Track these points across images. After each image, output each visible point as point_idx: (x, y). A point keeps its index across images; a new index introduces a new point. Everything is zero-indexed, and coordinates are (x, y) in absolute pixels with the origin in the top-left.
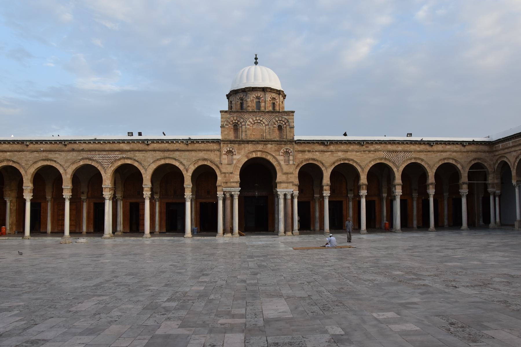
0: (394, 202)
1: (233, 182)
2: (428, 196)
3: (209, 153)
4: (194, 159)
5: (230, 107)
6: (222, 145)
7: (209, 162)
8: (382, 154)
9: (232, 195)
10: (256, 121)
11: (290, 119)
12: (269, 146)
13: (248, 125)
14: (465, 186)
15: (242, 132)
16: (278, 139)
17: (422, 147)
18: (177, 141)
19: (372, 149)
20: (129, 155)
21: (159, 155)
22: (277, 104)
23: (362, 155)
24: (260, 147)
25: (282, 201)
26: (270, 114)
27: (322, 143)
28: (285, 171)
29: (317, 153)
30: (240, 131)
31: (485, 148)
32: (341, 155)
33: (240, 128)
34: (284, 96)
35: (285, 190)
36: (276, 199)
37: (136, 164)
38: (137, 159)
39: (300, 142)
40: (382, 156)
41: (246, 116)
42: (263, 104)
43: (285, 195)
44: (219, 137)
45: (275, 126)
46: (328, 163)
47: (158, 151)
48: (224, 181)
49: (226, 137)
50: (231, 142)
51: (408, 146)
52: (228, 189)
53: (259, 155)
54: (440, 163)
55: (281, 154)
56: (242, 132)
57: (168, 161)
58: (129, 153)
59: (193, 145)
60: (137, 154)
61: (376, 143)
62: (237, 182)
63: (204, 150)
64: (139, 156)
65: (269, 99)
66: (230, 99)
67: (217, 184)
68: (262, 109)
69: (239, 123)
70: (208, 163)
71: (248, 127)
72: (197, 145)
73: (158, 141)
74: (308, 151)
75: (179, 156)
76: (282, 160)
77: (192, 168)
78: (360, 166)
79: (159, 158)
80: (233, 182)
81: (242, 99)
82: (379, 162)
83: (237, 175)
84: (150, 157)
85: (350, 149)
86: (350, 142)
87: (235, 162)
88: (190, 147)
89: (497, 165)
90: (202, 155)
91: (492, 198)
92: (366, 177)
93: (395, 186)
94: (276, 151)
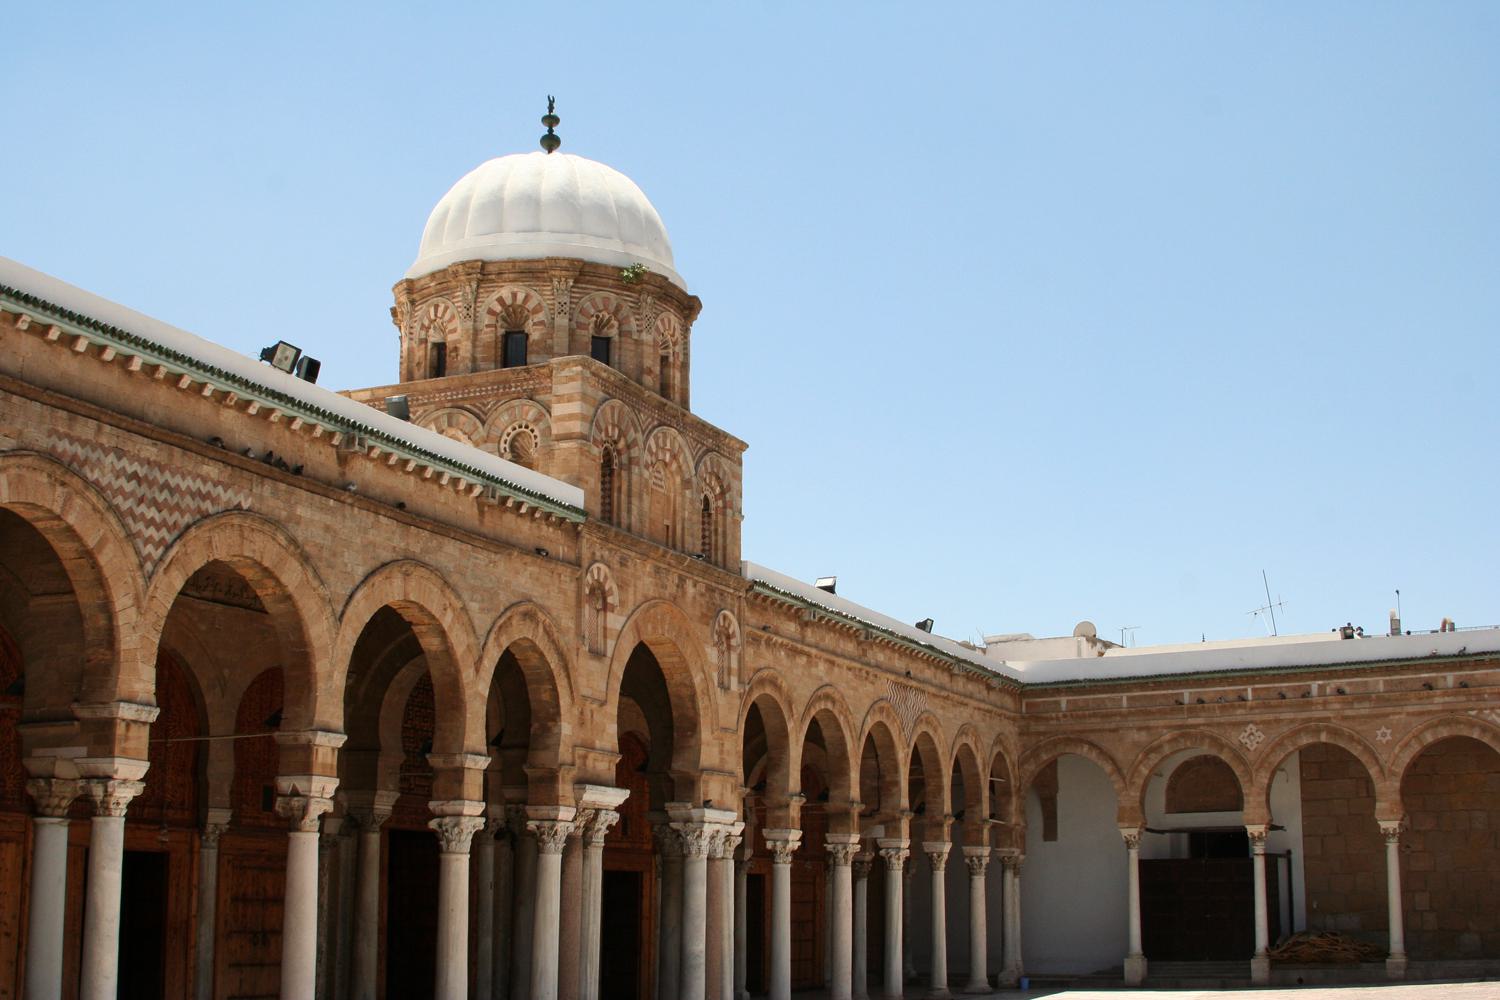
4: (504, 599)
7: (541, 630)
15: (629, 496)
21: (388, 536)
28: (723, 723)
30: (624, 488)
31: (1008, 701)
37: (292, 576)
38: (300, 534)
56: (629, 496)
69: (621, 444)
71: (646, 474)
72: (509, 519)
79: (386, 556)
84: (354, 539)
89: (1031, 767)
90: (523, 578)
91: (1009, 875)
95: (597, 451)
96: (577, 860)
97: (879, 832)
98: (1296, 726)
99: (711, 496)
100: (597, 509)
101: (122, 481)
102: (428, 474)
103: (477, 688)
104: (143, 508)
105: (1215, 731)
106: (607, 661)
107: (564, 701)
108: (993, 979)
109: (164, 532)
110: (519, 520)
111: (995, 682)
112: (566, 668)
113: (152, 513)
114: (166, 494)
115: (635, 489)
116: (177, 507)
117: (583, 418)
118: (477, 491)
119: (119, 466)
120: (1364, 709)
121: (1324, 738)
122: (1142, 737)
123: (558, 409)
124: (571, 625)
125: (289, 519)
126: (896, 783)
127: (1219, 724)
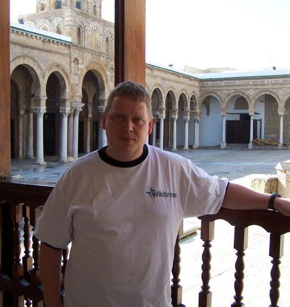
3: (61, 57)
4: (50, 63)
6: (72, 50)
8: (158, 80)
12: (102, 58)
14: (189, 114)
30: (83, 36)
31: (197, 84)
49: (74, 41)
62: (80, 96)
69: (82, 26)
71: (89, 33)
72: (51, 45)
79: (19, 55)
89: (202, 98)
90: (55, 58)
91: (196, 123)
93: (161, 111)
95: (75, 28)
96: (72, 119)
97: (158, 113)
98: (261, 90)
99: (108, 37)
100: (76, 42)
102: (29, 36)
103: (44, 82)
105: (243, 91)
106: (78, 76)
107: (67, 84)
108: (191, 147)
111: (191, 78)
115: (86, 36)
117: (71, 21)
118: (42, 39)
120: (277, 86)
121: (267, 93)
122: (227, 92)
123: (66, 19)
124: (69, 67)
126: (162, 102)
127: (244, 89)
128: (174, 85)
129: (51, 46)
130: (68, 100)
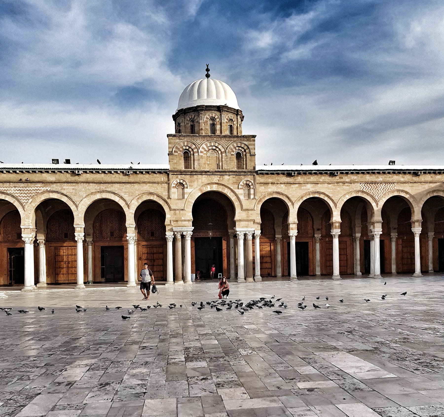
0: (372, 243)
1: (185, 220)
2: (412, 235)
5: (178, 130)
7: (155, 196)
8: (358, 187)
9: (184, 235)
10: (210, 148)
11: (250, 145)
12: (226, 177)
13: (201, 152)
16: (235, 169)
17: (408, 177)
18: (116, 171)
19: (348, 180)
20: (55, 187)
21: (93, 187)
22: (235, 127)
23: (334, 187)
24: (216, 179)
25: (241, 242)
26: (227, 139)
27: (289, 174)
29: (282, 185)
32: (310, 188)
33: (192, 156)
34: (242, 118)
35: (245, 229)
36: (232, 241)
37: (64, 199)
38: (65, 192)
39: (262, 173)
40: (359, 189)
41: (198, 141)
42: (218, 127)
43: (245, 235)
44: (166, 166)
45: (232, 153)
46: (295, 195)
47: (92, 183)
48: (174, 219)
49: (175, 166)
50: (181, 173)
51: (390, 176)
52: (179, 229)
53: (215, 188)
54: (429, 197)
55: (240, 187)
57: (105, 196)
58: (54, 185)
59: (135, 175)
60: (65, 186)
61: (352, 173)
62: (189, 220)
63: (149, 182)
64: (67, 189)
65: (226, 120)
66: (178, 121)
67: (166, 223)
68: (218, 133)
69: (190, 150)
70: (155, 198)
72: (140, 176)
73: (92, 171)
74: (272, 183)
75: (119, 189)
76: (241, 194)
77: (135, 204)
78: (333, 201)
79: (94, 191)
80: (185, 220)
81: (193, 121)
82: (354, 195)
83: (189, 212)
85: (321, 180)
86: (320, 173)
87: (186, 196)
88: (132, 178)
90: (146, 188)
92: (339, 213)
93: (373, 224)
94: (234, 183)
101: (17, 191)
104: (22, 195)
109: (28, 198)
110: (144, 175)
112: (167, 203)
113: (26, 195)
114: (27, 191)
116: (31, 193)
119: (15, 189)
125: (61, 189)
128: (407, 188)
129: (140, 177)
130: (169, 225)
